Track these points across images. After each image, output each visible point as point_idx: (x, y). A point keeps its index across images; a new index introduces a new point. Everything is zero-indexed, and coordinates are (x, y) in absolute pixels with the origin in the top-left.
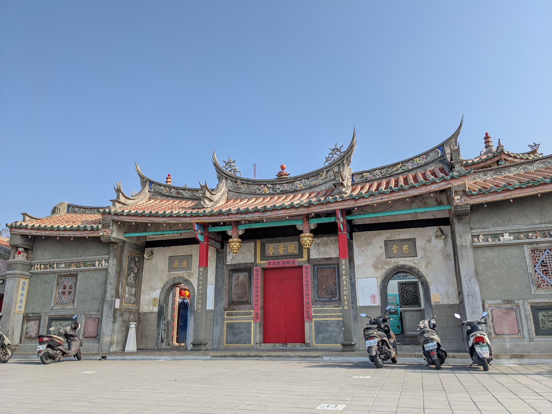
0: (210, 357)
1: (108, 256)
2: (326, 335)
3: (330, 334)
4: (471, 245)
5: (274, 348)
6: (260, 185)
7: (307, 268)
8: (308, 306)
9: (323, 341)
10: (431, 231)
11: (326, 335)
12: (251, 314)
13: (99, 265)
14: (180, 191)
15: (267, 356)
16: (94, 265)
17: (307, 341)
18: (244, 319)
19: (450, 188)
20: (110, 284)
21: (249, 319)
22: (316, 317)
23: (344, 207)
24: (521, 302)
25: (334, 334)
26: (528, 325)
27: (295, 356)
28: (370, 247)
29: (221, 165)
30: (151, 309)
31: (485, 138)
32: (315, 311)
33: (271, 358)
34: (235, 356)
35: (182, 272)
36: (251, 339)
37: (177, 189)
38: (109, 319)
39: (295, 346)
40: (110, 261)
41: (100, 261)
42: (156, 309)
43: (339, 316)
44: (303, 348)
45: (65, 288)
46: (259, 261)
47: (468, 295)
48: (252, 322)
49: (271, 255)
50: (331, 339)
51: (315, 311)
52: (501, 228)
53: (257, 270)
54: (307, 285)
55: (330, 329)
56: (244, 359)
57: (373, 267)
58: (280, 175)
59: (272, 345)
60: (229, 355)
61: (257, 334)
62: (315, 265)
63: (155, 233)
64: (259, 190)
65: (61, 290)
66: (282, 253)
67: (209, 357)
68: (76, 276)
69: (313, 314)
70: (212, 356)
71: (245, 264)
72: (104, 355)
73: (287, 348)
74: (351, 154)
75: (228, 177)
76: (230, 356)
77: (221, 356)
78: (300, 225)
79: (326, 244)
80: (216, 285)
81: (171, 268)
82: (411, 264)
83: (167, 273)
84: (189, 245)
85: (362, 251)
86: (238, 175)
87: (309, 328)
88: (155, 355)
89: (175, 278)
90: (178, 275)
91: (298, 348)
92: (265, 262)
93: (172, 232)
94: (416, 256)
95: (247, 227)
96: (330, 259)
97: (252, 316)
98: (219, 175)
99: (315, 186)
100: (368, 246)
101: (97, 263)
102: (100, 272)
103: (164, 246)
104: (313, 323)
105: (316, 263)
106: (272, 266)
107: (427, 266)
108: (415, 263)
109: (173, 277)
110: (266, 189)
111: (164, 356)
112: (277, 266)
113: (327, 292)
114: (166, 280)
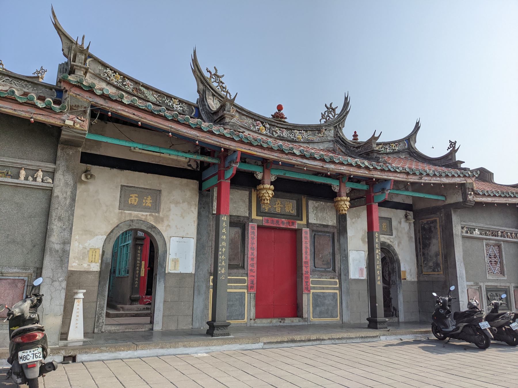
0: (262, 344)
1: (52, 166)
2: (323, 308)
3: (326, 308)
4: (461, 234)
5: (271, 325)
6: (256, 120)
7: (306, 232)
8: (307, 275)
9: (321, 315)
10: (401, 213)
11: (323, 308)
12: (243, 281)
13: (26, 179)
14: (142, 88)
15: (329, 339)
16: (18, 177)
17: (305, 315)
18: (236, 288)
19: (464, 184)
20: (60, 219)
21: (239, 287)
22: (314, 288)
23: (396, 179)
25: (330, 308)
27: (356, 338)
28: (360, 219)
30: (85, 265)
31: (353, 136)
32: (313, 282)
33: (333, 341)
34: (293, 341)
35: (144, 213)
36: (244, 314)
37: (136, 82)
38: (56, 284)
39: (293, 322)
40: (59, 176)
41: (32, 173)
42: (96, 267)
43: (334, 289)
44: (301, 323)
46: (254, 216)
47: (460, 277)
48: (246, 291)
49: (267, 211)
50: (327, 313)
51: (313, 282)
52: (474, 224)
53: (253, 228)
54: (306, 253)
55: (327, 302)
56: (304, 344)
57: (362, 240)
58: (278, 117)
59: (269, 320)
60: (286, 340)
61: (252, 308)
62: (313, 231)
63: (145, 147)
64: (254, 125)
66: (278, 210)
67: (261, 345)
69: (311, 285)
70: (265, 343)
71: (238, 217)
72: (72, 353)
73: (285, 324)
74: (345, 119)
76: (287, 342)
77: (277, 342)
78: (335, 184)
79: (323, 209)
80: (198, 240)
81: (124, 205)
82: (388, 242)
83: (117, 211)
84: (156, 176)
85: (353, 223)
87: (307, 301)
88: (178, 347)
89: (132, 221)
90: (137, 216)
91: (296, 324)
92: (260, 218)
93: (176, 153)
94: (392, 235)
95: (281, 173)
96: (327, 226)
97: (246, 284)
98: (201, 87)
99: (312, 142)
100: (358, 218)
101: (23, 173)
102: (28, 191)
103: (112, 167)
104: (311, 295)
105: (315, 228)
106: (270, 225)
107: (398, 245)
108: (391, 241)
109: (128, 218)
110: (262, 127)
111: (193, 347)
112: (275, 225)
113: (323, 261)
114: (115, 221)
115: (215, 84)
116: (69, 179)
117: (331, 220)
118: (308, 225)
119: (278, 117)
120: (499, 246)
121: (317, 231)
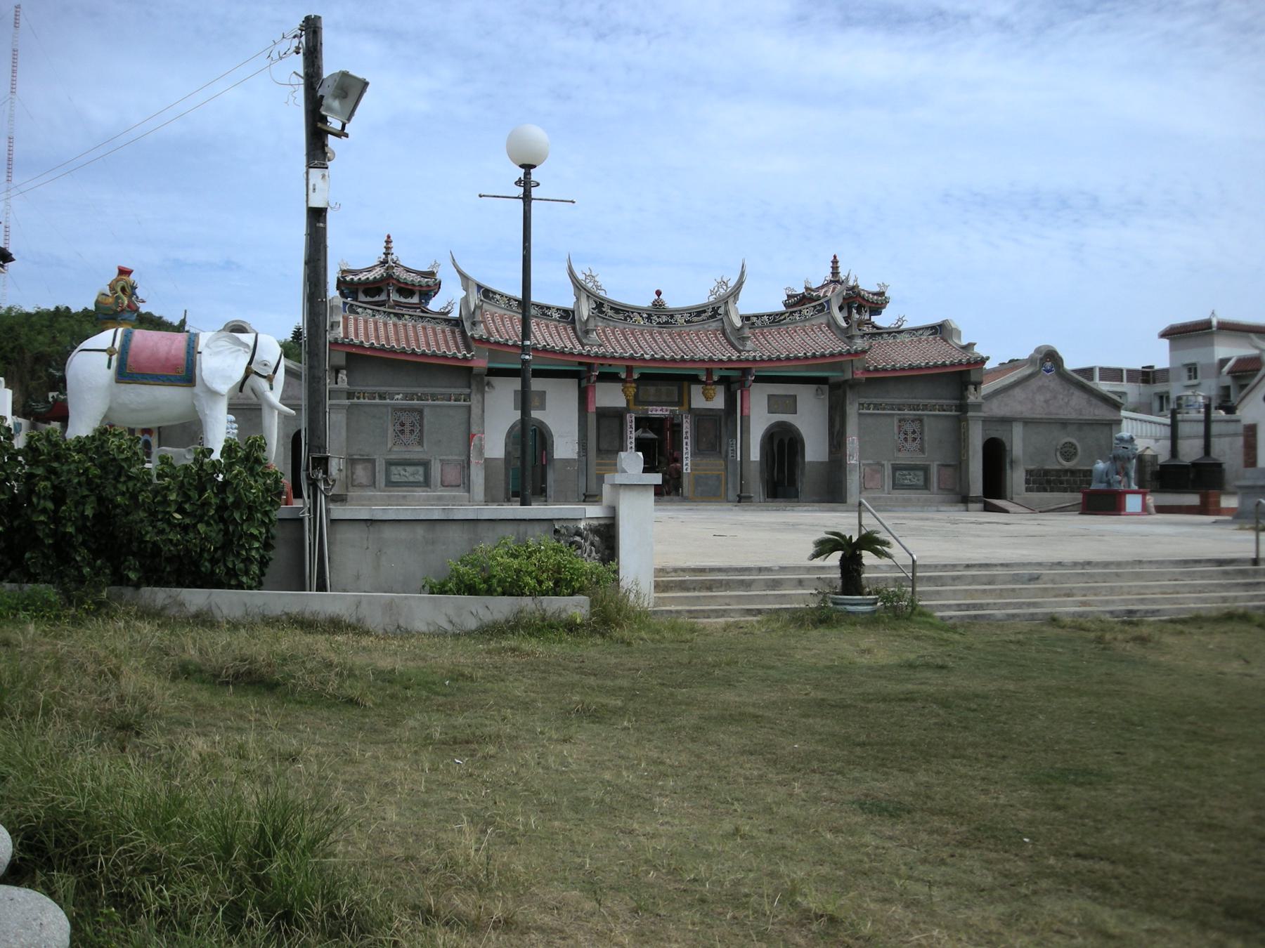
1: (468, 391)
10: (811, 388)
24: (885, 463)
26: (888, 482)
29: (581, 277)
40: (473, 396)
45: (402, 425)
58: (658, 306)
65: (398, 427)
68: (421, 412)
75: (590, 295)
86: (602, 293)
115: (590, 285)
116: (479, 397)
117: (718, 402)
118: (690, 410)
119: (658, 306)
120: (921, 421)
121: (701, 417)
